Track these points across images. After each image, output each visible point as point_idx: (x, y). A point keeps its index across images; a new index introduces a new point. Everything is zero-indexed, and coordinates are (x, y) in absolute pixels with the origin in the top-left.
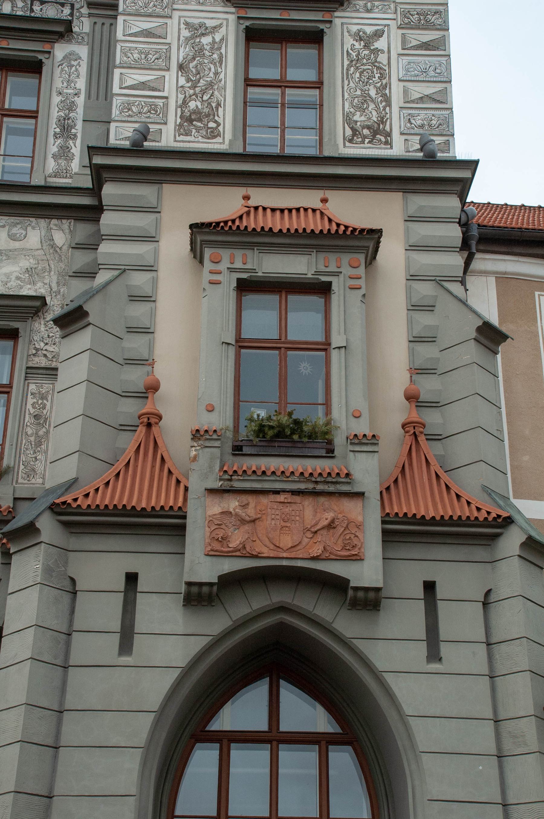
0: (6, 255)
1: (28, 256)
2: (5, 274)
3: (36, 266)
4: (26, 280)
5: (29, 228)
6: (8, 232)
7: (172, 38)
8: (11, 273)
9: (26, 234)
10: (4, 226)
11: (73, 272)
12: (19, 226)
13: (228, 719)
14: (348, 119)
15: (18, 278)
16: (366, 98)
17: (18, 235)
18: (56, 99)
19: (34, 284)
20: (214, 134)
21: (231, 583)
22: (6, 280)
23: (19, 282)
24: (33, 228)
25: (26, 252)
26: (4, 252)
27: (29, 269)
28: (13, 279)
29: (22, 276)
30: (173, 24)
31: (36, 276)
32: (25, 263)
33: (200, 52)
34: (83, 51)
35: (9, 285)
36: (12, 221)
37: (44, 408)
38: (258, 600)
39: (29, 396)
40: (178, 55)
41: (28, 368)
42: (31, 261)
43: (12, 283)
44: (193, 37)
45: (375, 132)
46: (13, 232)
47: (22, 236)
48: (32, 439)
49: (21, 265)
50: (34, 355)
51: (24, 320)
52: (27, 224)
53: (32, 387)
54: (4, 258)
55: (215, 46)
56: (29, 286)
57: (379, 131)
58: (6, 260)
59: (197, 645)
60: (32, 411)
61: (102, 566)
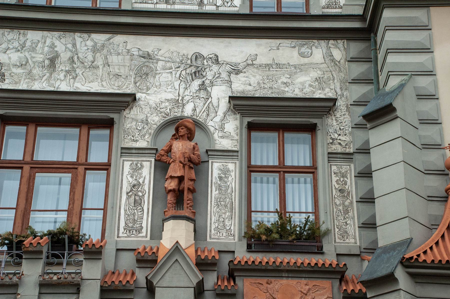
0: (300, 69)
1: (316, 68)
2: (301, 83)
3: (323, 76)
4: (317, 87)
5: (314, 48)
6: (299, 51)
8: (305, 82)
9: (312, 52)
10: (294, 47)
11: (352, 80)
12: (306, 46)
15: (310, 86)
17: (306, 53)
19: (323, 89)
22: (301, 87)
23: (312, 89)
24: (317, 47)
25: (313, 66)
26: (297, 66)
27: (318, 79)
28: (307, 86)
29: (313, 84)
31: (324, 84)
32: (315, 74)
35: (304, 91)
36: (300, 43)
37: (346, 184)
39: (333, 176)
41: (329, 153)
42: (319, 72)
43: (306, 89)
46: (302, 51)
47: (309, 53)
48: (341, 208)
49: (311, 75)
50: (331, 143)
51: (321, 117)
52: (312, 44)
53: (334, 168)
54: (298, 71)
56: (320, 91)
58: (299, 72)
60: (337, 186)
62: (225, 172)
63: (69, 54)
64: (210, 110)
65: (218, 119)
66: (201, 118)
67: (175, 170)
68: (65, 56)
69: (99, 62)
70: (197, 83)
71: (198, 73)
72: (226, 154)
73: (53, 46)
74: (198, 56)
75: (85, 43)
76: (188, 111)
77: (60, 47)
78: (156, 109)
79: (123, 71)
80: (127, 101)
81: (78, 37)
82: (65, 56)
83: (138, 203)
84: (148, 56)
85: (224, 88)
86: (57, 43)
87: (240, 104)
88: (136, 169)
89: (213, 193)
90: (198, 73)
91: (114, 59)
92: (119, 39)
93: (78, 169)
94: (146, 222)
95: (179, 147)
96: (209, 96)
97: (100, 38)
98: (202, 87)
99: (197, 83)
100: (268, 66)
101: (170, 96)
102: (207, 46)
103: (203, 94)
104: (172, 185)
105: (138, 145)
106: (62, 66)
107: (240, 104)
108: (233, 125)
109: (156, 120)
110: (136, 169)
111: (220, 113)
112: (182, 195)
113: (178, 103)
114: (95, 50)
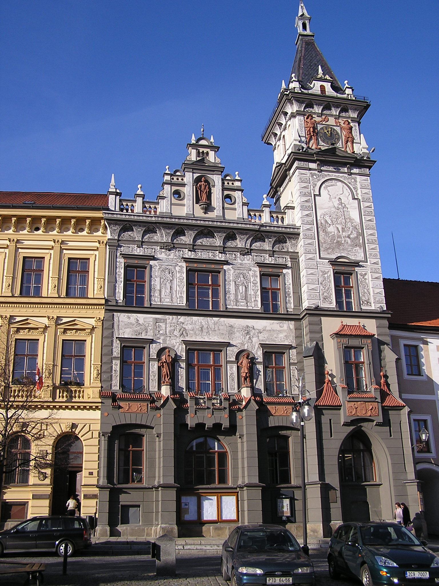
16: (364, 293)
44: (323, 274)
45: (368, 303)
57: (368, 303)
63: (207, 326)
64: (253, 347)
65: (255, 350)
66: (250, 350)
68: (205, 326)
69: (216, 329)
70: (248, 336)
71: (248, 333)
73: (201, 323)
74: (248, 326)
76: (246, 348)
77: (203, 323)
79: (224, 332)
82: (205, 326)
83: (233, 380)
84: (231, 326)
85: (256, 338)
86: (202, 321)
88: (231, 368)
90: (248, 333)
91: (221, 327)
92: (222, 319)
96: (252, 341)
99: (248, 336)
101: (240, 342)
103: (250, 341)
105: (231, 360)
106: (205, 331)
107: (263, 346)
111: (256, 348)
113: (243, 344)
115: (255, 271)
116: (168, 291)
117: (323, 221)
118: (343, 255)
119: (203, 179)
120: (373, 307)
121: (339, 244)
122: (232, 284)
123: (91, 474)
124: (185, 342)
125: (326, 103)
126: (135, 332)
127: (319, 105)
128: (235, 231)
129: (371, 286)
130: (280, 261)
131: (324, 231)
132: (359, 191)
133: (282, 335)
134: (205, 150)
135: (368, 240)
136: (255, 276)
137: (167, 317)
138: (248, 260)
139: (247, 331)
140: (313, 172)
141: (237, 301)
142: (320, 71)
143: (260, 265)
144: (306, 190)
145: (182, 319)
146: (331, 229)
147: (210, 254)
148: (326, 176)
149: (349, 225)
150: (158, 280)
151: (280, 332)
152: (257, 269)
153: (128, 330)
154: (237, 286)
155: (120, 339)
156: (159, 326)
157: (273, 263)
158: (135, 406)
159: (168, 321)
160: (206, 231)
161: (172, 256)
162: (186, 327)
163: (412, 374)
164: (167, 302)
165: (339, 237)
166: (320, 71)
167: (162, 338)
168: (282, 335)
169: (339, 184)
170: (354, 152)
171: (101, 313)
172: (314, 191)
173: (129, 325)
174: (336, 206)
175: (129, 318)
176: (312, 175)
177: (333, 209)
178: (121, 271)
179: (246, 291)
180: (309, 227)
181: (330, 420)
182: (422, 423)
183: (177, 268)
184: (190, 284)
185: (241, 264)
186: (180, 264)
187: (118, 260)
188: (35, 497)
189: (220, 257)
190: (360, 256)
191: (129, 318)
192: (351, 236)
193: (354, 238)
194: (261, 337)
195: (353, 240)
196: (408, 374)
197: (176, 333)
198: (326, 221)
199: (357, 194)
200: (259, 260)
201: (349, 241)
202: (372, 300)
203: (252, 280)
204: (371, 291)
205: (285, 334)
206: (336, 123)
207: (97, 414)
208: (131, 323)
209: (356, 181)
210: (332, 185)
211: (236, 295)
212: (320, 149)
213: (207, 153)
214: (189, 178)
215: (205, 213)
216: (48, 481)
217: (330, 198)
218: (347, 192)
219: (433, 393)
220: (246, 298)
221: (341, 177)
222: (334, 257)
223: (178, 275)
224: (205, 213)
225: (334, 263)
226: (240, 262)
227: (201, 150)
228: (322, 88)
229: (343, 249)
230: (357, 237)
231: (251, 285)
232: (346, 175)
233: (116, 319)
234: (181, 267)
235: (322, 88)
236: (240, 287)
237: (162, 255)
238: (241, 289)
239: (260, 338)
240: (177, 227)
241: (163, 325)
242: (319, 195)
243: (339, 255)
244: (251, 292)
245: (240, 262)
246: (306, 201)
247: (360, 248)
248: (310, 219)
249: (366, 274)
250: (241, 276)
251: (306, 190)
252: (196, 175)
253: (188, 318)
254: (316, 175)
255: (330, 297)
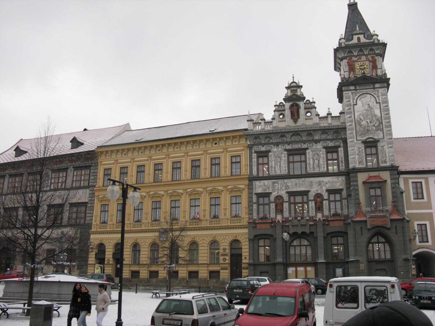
7: (356, 150)
13: (372, 241)
14: (381, 160)
16: (383, 156)
18: (340, 157)
20: (363, 164)
21: (373, 228)
30: (356, 148)
33: (360, 151)
34: (342, 149)
38: (377, 229)
40: (357, 153)
55: (362, 150)
57: (385, 162)
59: (370, 235)
61: (358, 228)
62: (326, 203)
66: (321, 193)
67: (318, 204)
68: (298, 183)
72: (326, 200)
74: (320, 181)
75: (301, 180)
76: (319, 192)
77: (297, 182)
78: (314, 192)
80: (308, 191)
81: (300, 179)
82: (298, 183)
83: (313, 209)
84: (311, 182)
87: (327, 190)
88: (312, 203)
89: (324, 207)
90: (320, 185)
91: (306, 183)
92: (306, 179)
93: (303, 203)
94: (314, 213)
95: (319, 200)
97: (303, 179)
98: (321, 187)
100: (332, 182)
102: (321, 179)
104: (318, 206)
106: (298, 185)
107: (327, 190)
108: (326, 194)
109: (314, 194)
110: (312, 203)
112: (319, 208)
113: (317, 190)
114: (303, 181)
115: (323, 151)
116: (279, 167)
117: (359, 119)
118: (370, 136)
119: (295, 105)
120: (388, 164)
121: (368, 130)
122: (311, 160)
123: (245, 258)
124: (287, 192)
125: (359, 49)
126: (264, 189)
127: (355, 51)
128: (311, 132)
129: (387, 152)
130: (337, 144)
131: (360, 125)
132: (380, 98)
133: (338, 184)
134: (295, 89)
135: (386, 126)
136: (323, 154)
137: (279, 180)
138: (319, 146)
139: (320, 184)
140: (353, 91)
141: (314, 168)
142: (358, 28)
143: (324, 148)
144: (348, 103)
145: (286, 181)
146: (364, 123)
147: (299, 145)
148: (360, 92)
149: (374, 118)
150: (273, 162)
151: (338, 182)
152: (324, 150)
153: (260, 189)
154: (314, 161)
155: (257, 194)
156: (275, 186)
157: (333, 145)
158: (263, 226)
159: (279, 182)
160: (296, 133)
161: (280, 149)
162: (288, 185)
163: (418, 199)
164: (278, 173)
165: (368, 126)
166: (358, 28)
167: (277, 191)
168: (338, 184)
169: (369, 96)
170: (377, 75)
171: (247, 182)
172: (353, 102)
173: (260, 186)
174: (366, 109)
175: (260, 183)
176: (352, 93)
177: (365, 111)
178: (255, 160)
179: (319, 163)
180: (350, 124)
181: (361, 228)
182: (423, 227)
183: (283, 155)
184: (289, 162)
185: (316, 148)
186: (284, 153)
187: (253, 154)
188: (222, 269)
189: (304, 146)
190: (381, 136)
191: (260, 183)
192: (376, 125)
193: (378, 126)
194: (327, 186)
195: (376, 127)
196: (414, 199)
197: (283, 188)
198: (361, 119)
199: (379, 100)
200: (325, 145)
201: (374, 128)
202: (387, 160)
203: (322, 156)
204: (387, 155)
205: (340, 183)
206: (366, 58)
207: (246, 231)
208: (261, 185)
209: (378, 92)
210: (364, 97)
211: (313, 165)
212: (357, 77)
213: (296, 90)
214: (287, 105)
215: (296, 123)
216: (227, 261)
217: (363, 105)
218: (373, 100)
219: (431, 208)
220: (319, 166)
221: (370, 91)
222: (364, 138)
223: (283, 158)
224: (296, 123)
225: (364, 142)
226: (315, 147)
227: (293, 89)
228: (359, 39)
229: (371, 133)
230: (379, 125)
231: (321, 160)
232: (372, 90)
233: (254, 184)
234: (285, 154)
235: (359, 39)
236: (316, 161)
237: (275, 149)
238: (316, 162)
239: (327, 186)
240: (281, 134)
241: (277, 185)
242: (356, 104)
243: (368, 137)
244: (321, 163)
245: (315, 147)
246: (349, 109)
247: (381, 131)
248: (351, 119)
249: (384, 146)
250: (316, 155)
251: (348, 103)
252: (290, 103)
253: (289, 180)
254: (354, 93)
255: (362, 161)
